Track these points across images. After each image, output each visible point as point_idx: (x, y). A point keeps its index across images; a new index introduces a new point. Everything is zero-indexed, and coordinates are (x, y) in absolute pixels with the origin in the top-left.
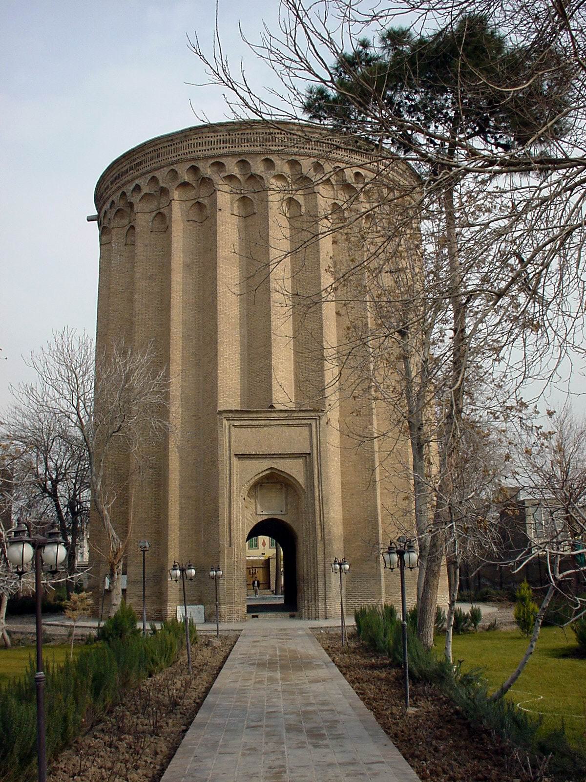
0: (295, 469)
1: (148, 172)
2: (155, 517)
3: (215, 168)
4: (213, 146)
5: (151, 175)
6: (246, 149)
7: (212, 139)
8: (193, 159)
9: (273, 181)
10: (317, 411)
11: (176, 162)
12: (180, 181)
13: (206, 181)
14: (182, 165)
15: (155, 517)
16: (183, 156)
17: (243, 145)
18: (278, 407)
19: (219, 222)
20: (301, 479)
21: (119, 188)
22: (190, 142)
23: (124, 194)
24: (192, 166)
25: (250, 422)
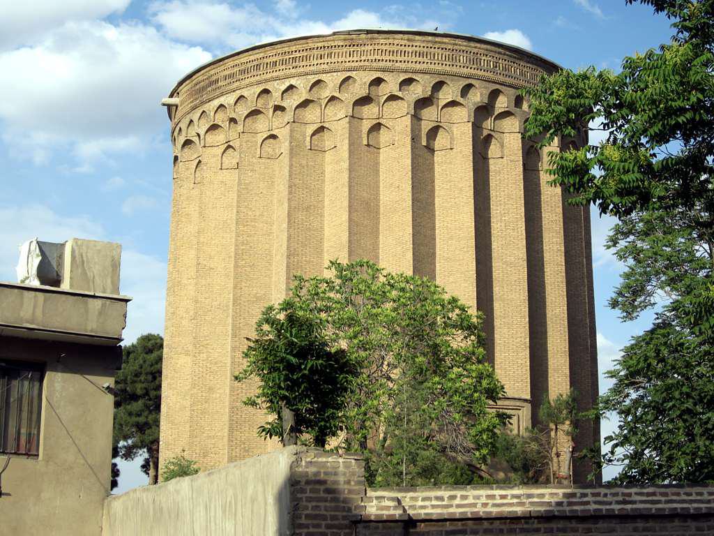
4: (406, 58)
6: (448, 68)
7: (407, 49)
11: (355, 69)
16: (366, 63)
17: (445, 63)
22: (377, 47)
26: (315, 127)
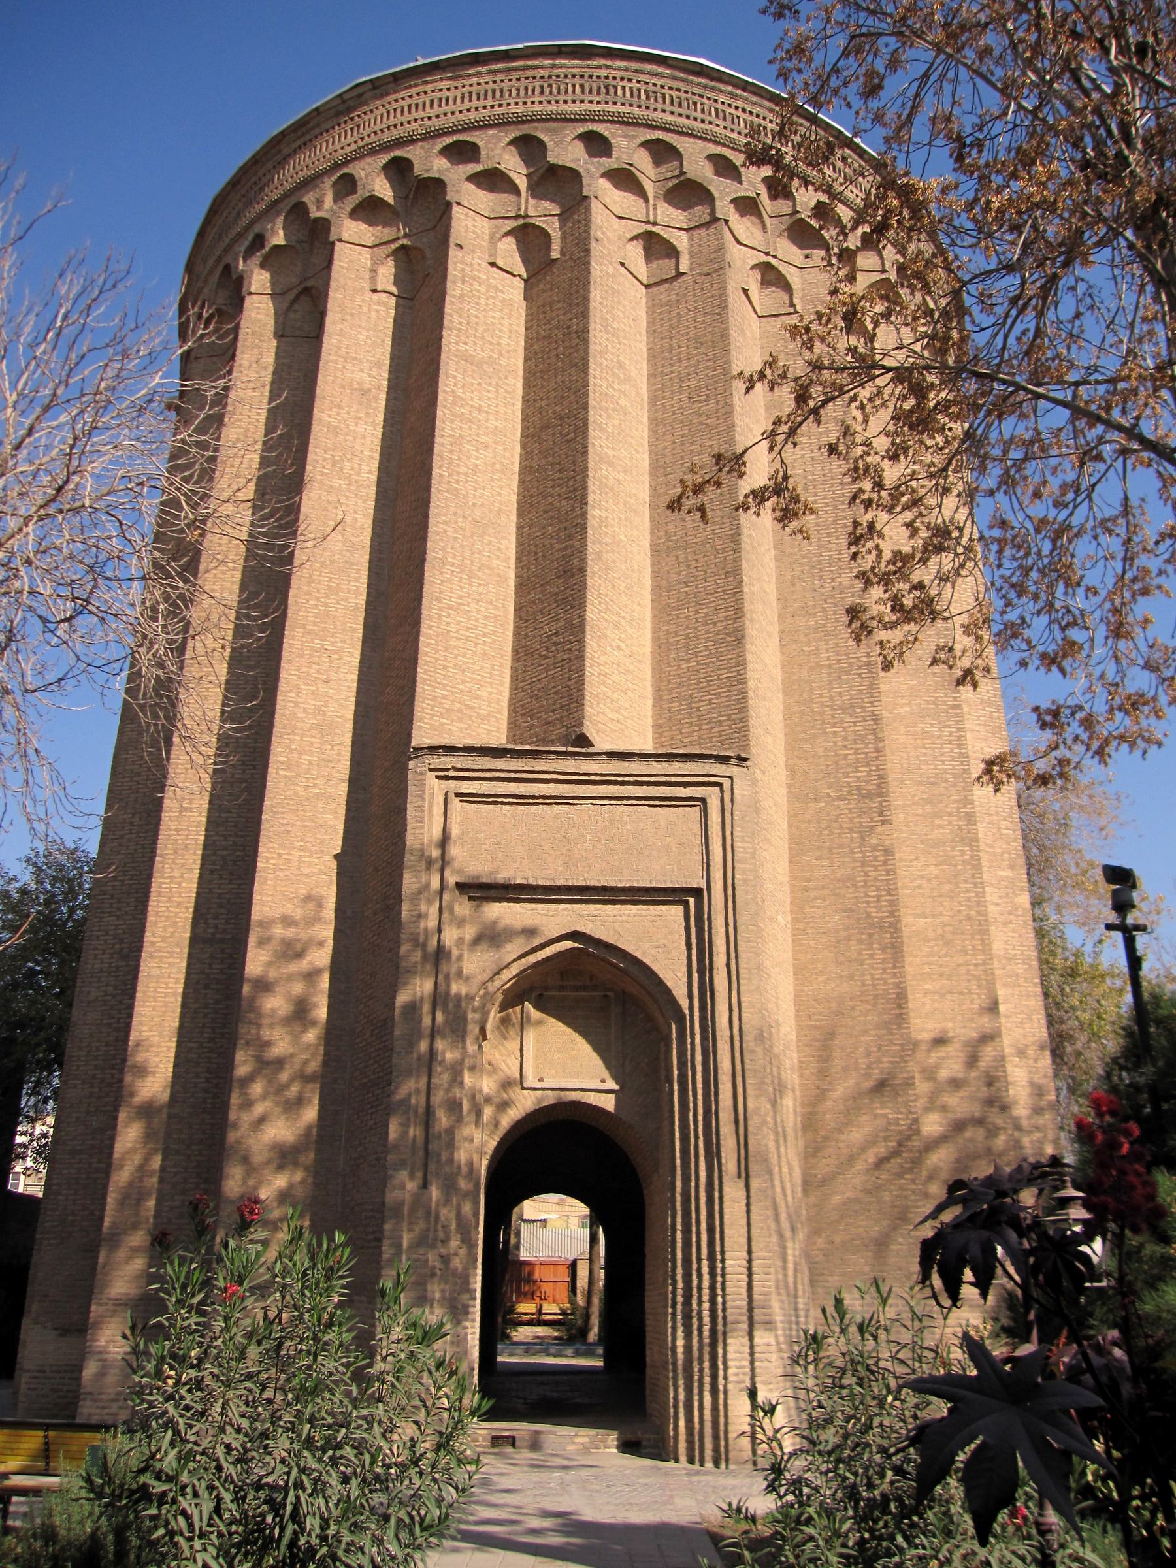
0: (654, 940)
1: (285, 196)
2: (206, 1091)
5: (292, 200)
8: (399, 143)
9: (604, 184)
10: (724, 759)
12: (361, 194)
14: (369, 160)
15: (206, 1091)
18: (602, 743)
20: (675, 976)
21: (220, 259)
24: (395, 160)
25: (513, 788)
26: (299, 289)
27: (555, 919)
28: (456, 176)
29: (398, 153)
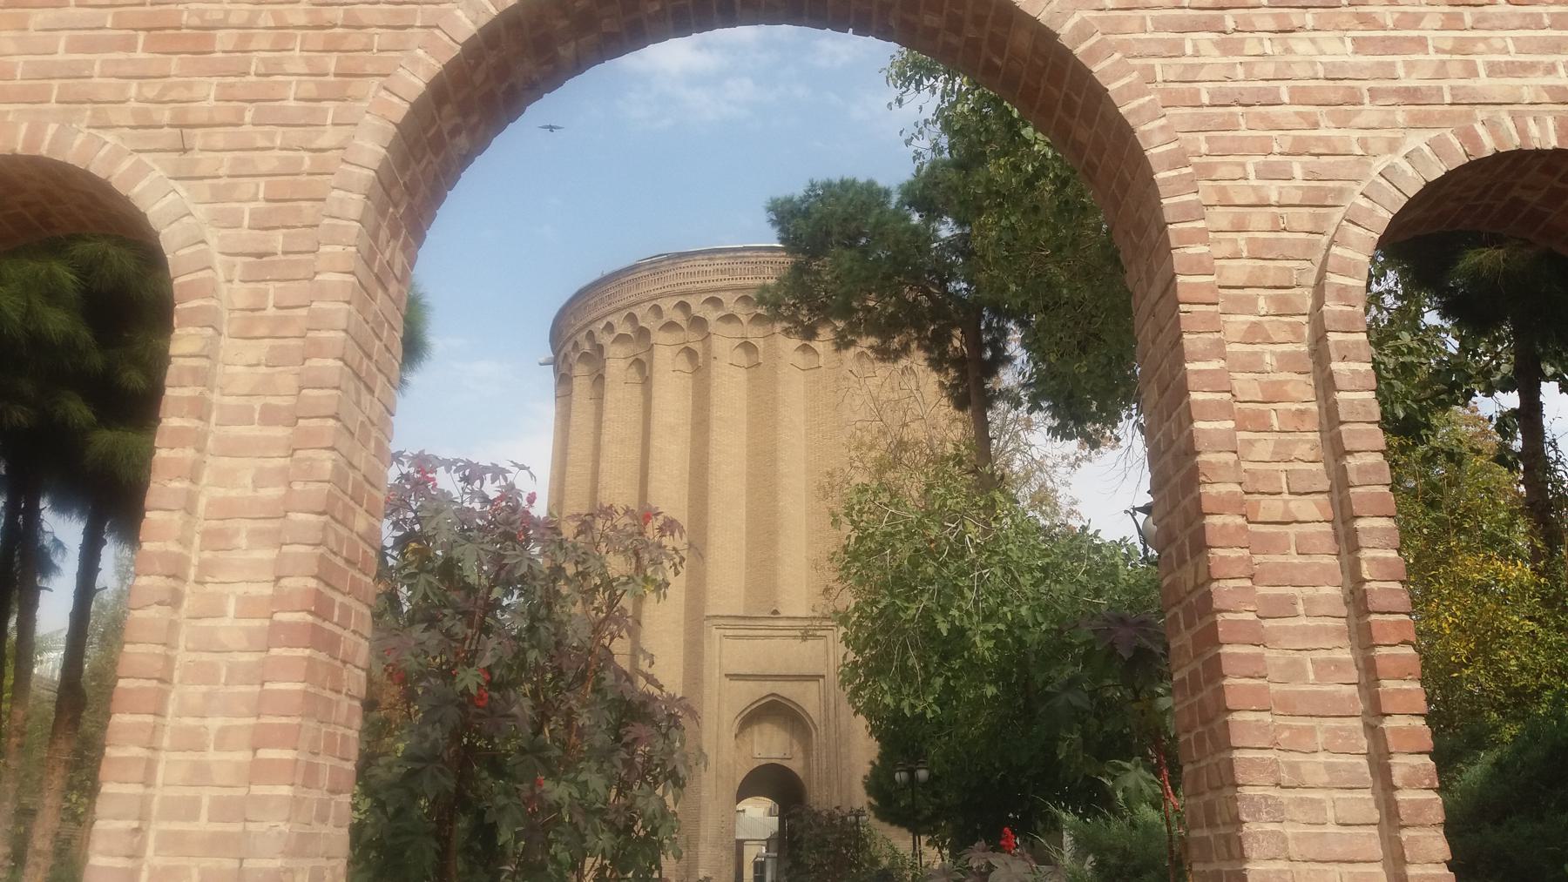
3: (709, 307)
11: (661, 296)
12: (665, 319)
13: (698, 323)
19: (713, 373)
23: (591, 334)
27: (768, 687)
28: (711, 315)
29: (682, 299)
